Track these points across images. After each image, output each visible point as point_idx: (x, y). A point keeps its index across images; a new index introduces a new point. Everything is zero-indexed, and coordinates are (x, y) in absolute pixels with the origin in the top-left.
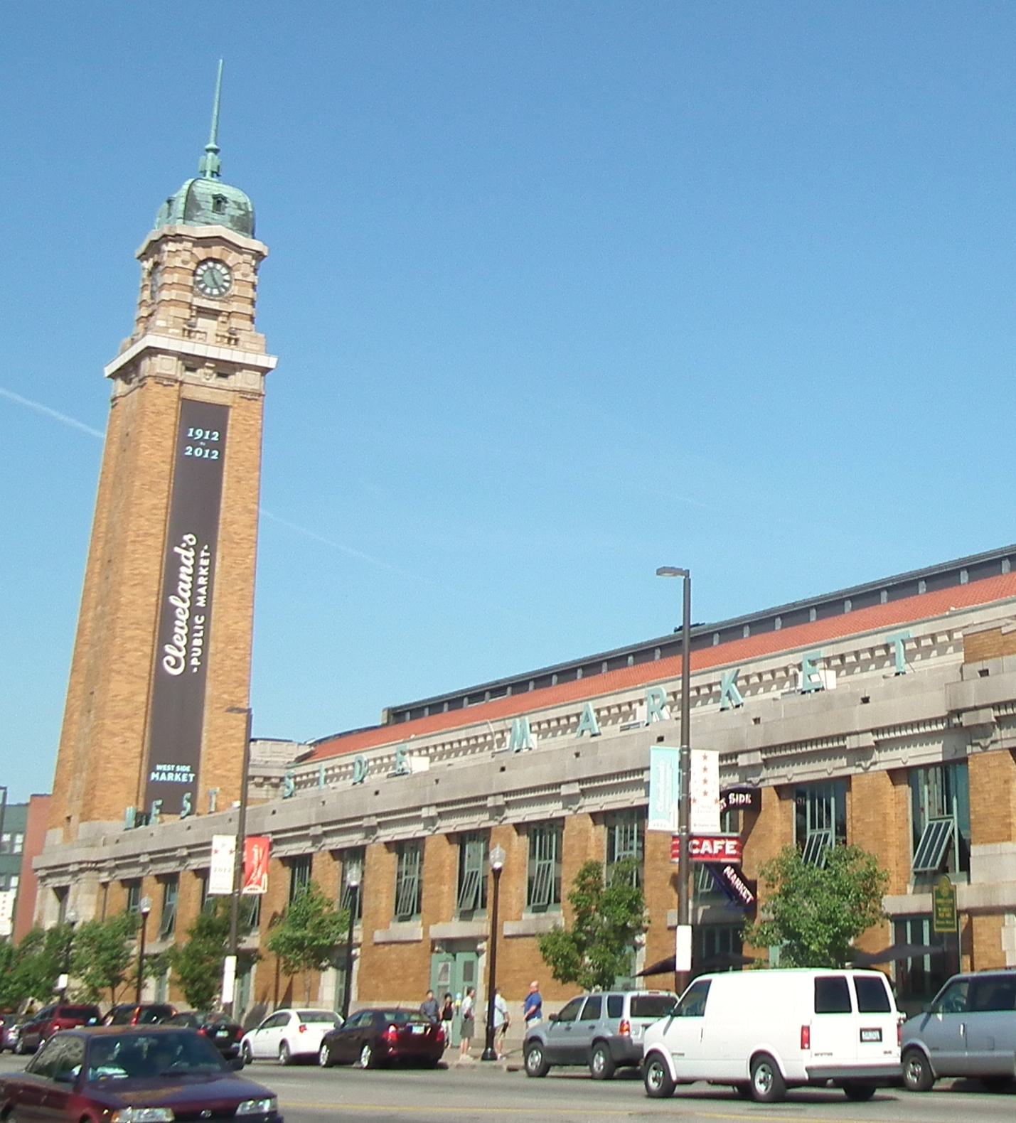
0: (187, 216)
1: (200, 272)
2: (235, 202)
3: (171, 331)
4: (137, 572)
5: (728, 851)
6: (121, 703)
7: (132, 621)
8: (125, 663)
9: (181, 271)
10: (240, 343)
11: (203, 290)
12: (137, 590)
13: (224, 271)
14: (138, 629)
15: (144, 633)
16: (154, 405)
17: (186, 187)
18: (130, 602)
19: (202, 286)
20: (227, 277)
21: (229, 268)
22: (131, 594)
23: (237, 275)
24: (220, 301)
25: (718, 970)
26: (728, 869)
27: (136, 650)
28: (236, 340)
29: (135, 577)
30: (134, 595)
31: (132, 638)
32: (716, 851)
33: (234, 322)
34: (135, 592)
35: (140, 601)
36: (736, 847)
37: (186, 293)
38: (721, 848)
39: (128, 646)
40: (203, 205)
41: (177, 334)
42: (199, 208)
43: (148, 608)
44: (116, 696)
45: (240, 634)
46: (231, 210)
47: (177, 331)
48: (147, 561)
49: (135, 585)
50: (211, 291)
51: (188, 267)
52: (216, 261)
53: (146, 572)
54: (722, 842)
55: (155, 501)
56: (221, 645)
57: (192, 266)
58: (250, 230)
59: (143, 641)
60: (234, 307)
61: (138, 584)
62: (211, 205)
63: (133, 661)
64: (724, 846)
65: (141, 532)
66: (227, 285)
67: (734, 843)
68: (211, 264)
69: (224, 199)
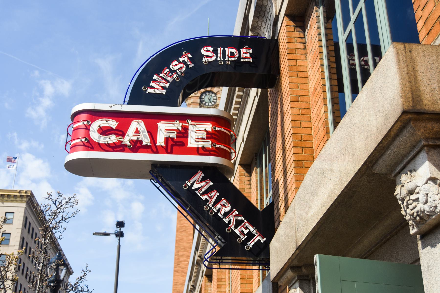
4: (183, 225)
5: (192, 143)
6: (180, 286)
7: (182, 248)
9: (194, 97)
11: (205, 104)
12: (184, 234)
13: (213, 95)
14: (185, 251)
15: (188, 253)
18: (181, 239)
19: (204, 103)
20: (215, 98)
21: (216, 94)
22: (181, 236)
24: (212, 107)
26: (200, 175)
29: (182, 228)
30: (182, 236)
31: (182, 256)
32: (161, 141)
34: (182, 234)
35: (185, 238)
36: (210, 136)
38: (173, 135)
39: (181, 259)
43: (190, 241)
44: (177, 283)
49: (182, 231)
50: (208, 104)
51: (197, 95)
52: (209, 92)
54: (177, 125)
61: (184, 231)
63: (184, 266)
64: (186, 129)
66: (215, 101)
67: (209, 127)
68: (207, 94)
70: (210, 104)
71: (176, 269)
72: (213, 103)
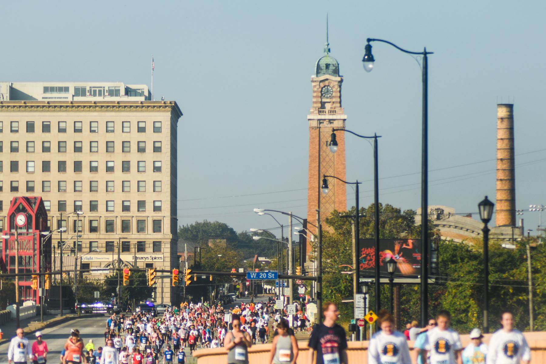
0: (318, 73)
2: (332, 64)
3: (315, 112)
8: (311, 212)
10: (336, 112)
11: (324, 96)
12: (312, 191)
16: (312, 136)
17: (317, 63)
20: (331, 90)
23: (334, 89)
25: (506, 249)
27: (314, 208)
28: (335, 111)
33: (334, 105)
37: (318, 99)
40: (323, 68)
41: (316, 113)
42: (321, 69)
45: (343, 201)
46: (331, 68)
48: (314, 183)
52: (328, 86)
53: (314, 186)
55: (315, 165)
56: (338, 205)
57: (320, 90)
58: (338, 72)
59: (315, 206)
60: (334, 100)
65: (312, 174)
66: (331, 93)
69: (329, 65)
70: (328, 96)
71: (309, 213)
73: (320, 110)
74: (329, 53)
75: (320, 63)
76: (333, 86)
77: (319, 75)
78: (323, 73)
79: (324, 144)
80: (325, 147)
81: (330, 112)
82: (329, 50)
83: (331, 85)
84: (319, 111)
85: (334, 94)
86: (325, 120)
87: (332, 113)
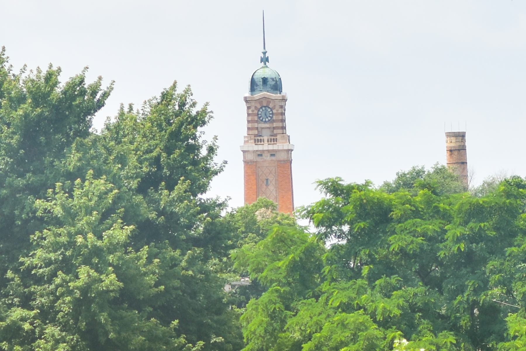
1: (260, 113)
11: (262, 120)
13: (269, 110)
20: (271, 112)
23: (274, 111)
28: (276, 139)
42: (257, 85)
47: (252, 141)
52: (265, 107)
60: (275, 125)
62: (261, 83)
68: (264, 109)
70: (267, 120)
72: (269, 118)
73: (256, 138)
74: (267, 62)
75: (254, 77)
76: (274, 107)
77: (254, 93)
78: (259, 89)
79: (263, 182)
80: (265, 187)
81: (269, 140)
82: (267, 60)
83: (271, 106)
84: (255, 140)
85: (274, 118)
86: (263, 151)
87: (272, 143)
